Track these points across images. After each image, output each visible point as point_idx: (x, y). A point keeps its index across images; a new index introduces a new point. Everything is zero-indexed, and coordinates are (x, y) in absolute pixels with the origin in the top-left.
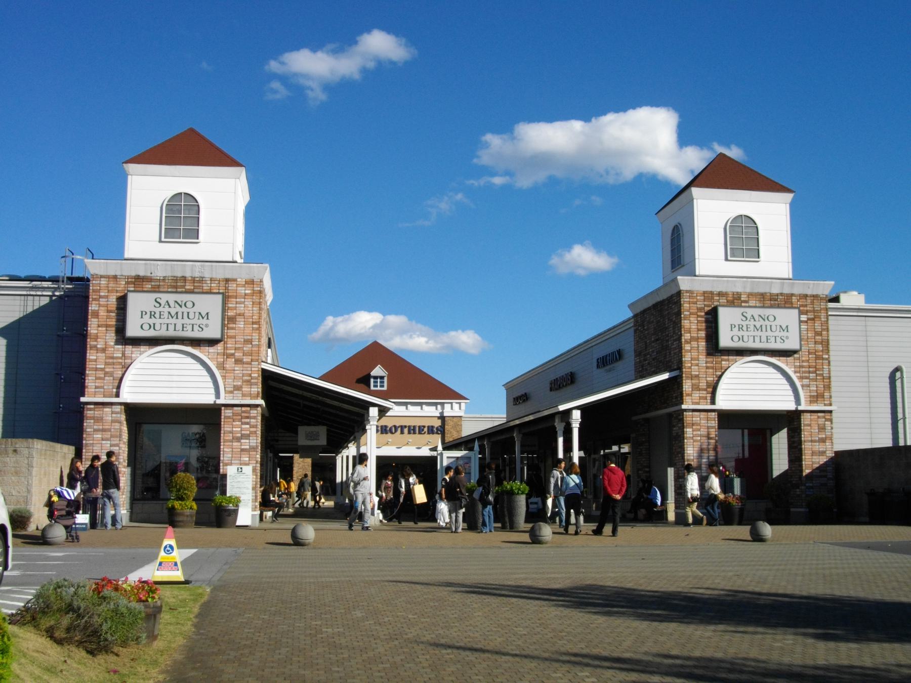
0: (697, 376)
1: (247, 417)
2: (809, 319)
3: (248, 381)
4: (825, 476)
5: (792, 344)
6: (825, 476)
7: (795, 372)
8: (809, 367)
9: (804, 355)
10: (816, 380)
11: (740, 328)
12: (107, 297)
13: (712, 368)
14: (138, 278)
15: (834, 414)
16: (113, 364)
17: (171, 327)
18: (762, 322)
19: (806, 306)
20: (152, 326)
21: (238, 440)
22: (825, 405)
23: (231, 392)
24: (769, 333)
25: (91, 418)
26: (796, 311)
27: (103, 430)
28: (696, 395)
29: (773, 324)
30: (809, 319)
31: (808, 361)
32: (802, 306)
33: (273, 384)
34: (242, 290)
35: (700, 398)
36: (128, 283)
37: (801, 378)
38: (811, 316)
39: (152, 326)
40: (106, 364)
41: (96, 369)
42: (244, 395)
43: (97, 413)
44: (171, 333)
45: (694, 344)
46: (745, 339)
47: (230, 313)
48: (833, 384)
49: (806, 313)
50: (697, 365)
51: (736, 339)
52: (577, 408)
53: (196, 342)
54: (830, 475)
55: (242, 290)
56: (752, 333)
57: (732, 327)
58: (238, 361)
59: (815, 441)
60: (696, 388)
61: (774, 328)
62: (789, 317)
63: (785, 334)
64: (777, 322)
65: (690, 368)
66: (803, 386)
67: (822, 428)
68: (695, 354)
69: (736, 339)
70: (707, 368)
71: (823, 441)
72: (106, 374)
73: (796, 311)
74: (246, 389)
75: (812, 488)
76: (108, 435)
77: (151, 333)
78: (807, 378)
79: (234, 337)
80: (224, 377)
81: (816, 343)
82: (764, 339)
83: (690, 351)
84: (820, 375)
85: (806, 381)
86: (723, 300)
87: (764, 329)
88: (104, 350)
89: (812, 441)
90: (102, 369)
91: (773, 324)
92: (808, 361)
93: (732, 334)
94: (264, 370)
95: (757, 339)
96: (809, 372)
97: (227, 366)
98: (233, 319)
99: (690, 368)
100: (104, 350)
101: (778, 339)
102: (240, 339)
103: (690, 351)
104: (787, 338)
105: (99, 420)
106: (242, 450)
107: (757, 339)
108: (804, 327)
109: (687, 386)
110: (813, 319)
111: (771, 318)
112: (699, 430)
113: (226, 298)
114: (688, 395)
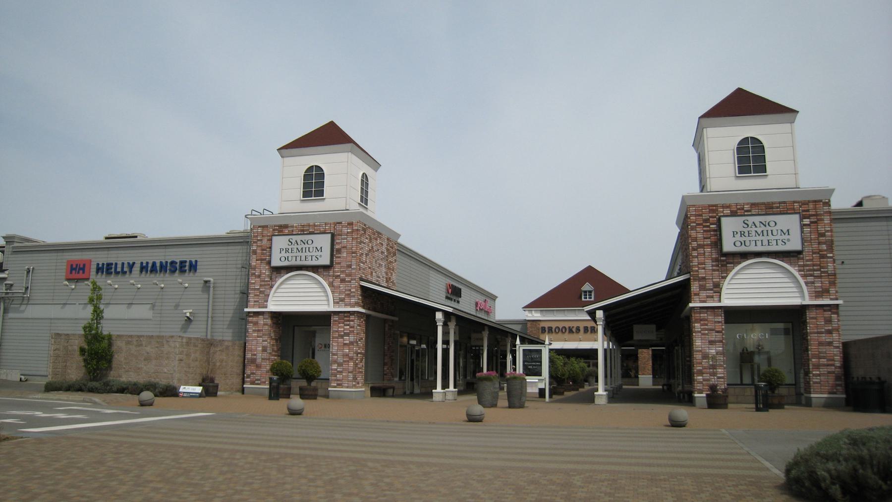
0: (704, 279)
1: (349, 321)
2: (811, 222)
3: (348, 295)
4: (833, 365)
5: (794, 244)
6: (833, 365)
7: (800, 271)
8: (814, 265)
9: (807, 255)
10: (820, 277)
11: (287, 251)
12: (261, 240)
13: (718, 270)
14: (280, 226)
15: (841, 308)
16: (265, 285)
17: (298, 259)
18: (763, 228)
19: (808, 211)
20: (287, 259)
21: (342, 337)
22: (831, 299)
23: (338, 303)
24: (771, 237)
25: (251, 322)
26: (797, 217)
27: (259, 331)
28: (703, 294)
29: (311, 246)
30: (811, 222)
31: (811, 260)
32: (804, 211)
33: (370, 296)
34: (345, 230)
35: (708, 297)
36: (274, 230)
37: (802, 276)
38: (813, 219)
39: (287, 259)
40: (261, 285)
41: (255, 289)
42: (346, 305)
43: (254, 319)
44: (299, 263)
45: (701, 251)
46: (747, 243)
47: (337, 247)
48: (838, 281)
49: (808, 217)
50: (704, 268)
51: (738, 244)
52: (599, 308)
53: (315, 269)
54: (838, 364)
55: (345, 230)
56: (295, 254)
57: (734, 234)
58: (343, 281)
59: (821, 333)
60: (703, 288)
61: (775, 233)
62: (791, 223)
63: (786, 237)
64: (778, 227)
65: (697, 271)
66: (806, 283)
67: (829, 321)
68: (701, 259)
69: (738, 244)
70: (714, 270)
71: (829, 332)
72: (261, 292)
73: (797, 217)
74: (347, 300)
75: (819, 375)
76: (261, 334)
77: (286, 263)
78: (811, 275)
79: (339, 263)
80: (333, 292)
81: (819, 243)
82: (303, 258)
83: (697, 257)
84: (824, 272)
85: (810, 279)
86: (727, 211)
87: (765, 233)
88: (259, 276)
89: (818, 333)
90: (258, 289)
91: (311, 246)
92: (811, 260)
93: (734, 239)
94: (362, 287)
95: (759, 243)
96: (814, 270)
97: (335, 284)
98: (339, 251)
99: (697, 271)
100: (259, 276)
101: (780, 242)
102: (344, 264)
103: (697, 257)
104: (788, 240)
105: (256, 324)
106: (345, 344)
107: (759, 243)
108: (807, 230)
109: (695, 287)
110: (815, 222)
111: (772, 224)
112: (706, 325)
113: (333, 236)
114: (695, 294)
